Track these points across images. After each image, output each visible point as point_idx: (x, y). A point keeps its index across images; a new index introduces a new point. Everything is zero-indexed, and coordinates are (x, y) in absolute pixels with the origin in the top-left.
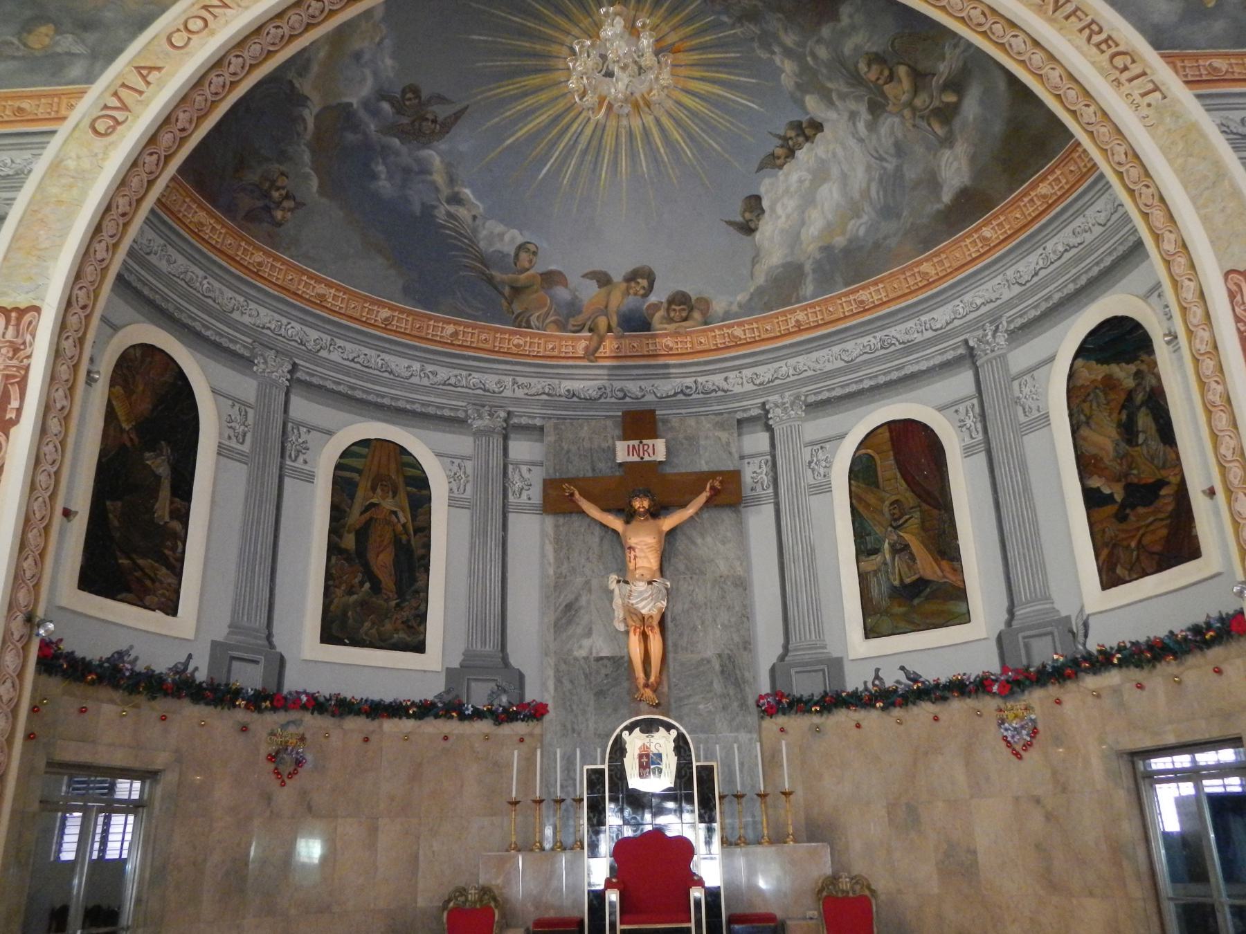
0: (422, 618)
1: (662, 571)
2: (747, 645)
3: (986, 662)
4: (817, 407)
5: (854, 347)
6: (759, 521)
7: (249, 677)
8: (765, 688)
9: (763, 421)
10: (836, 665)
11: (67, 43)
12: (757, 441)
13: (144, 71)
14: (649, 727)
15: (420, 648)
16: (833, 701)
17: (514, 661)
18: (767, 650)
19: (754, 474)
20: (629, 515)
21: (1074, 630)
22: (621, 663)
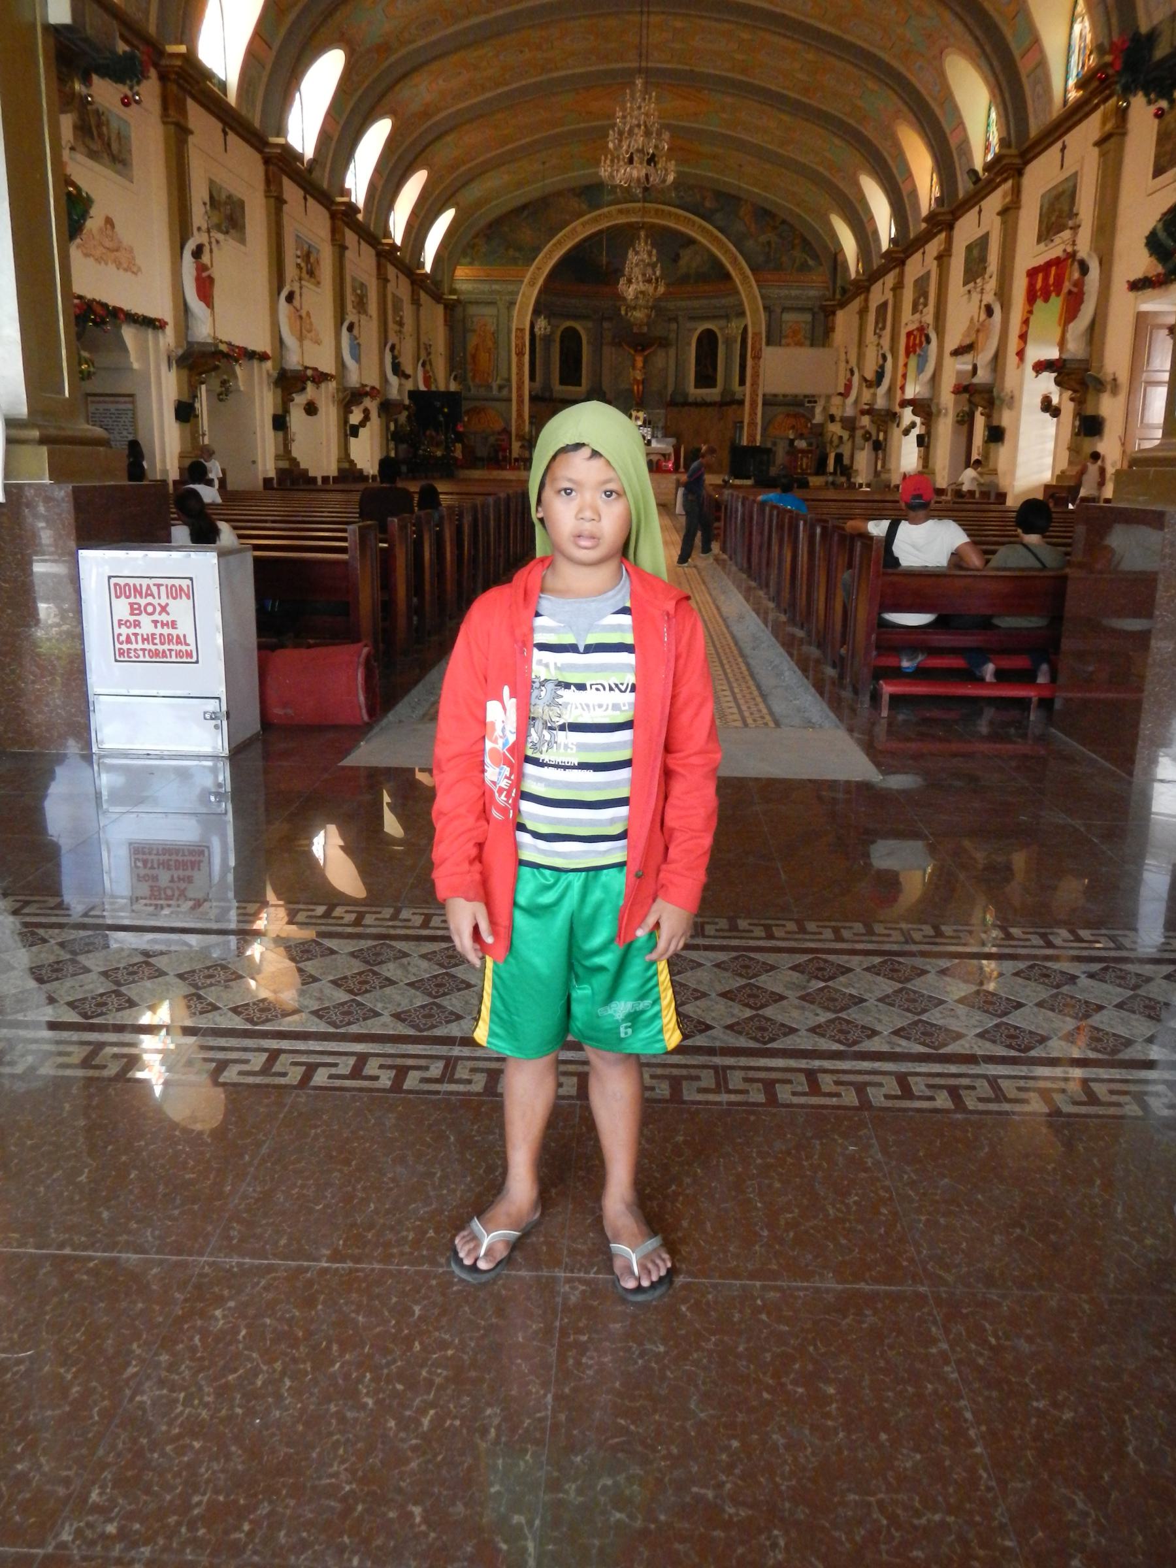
0: (580, 377)
1: (644, 367)
2: (666, 387)
3: (717, 398)
4: (692, 319)
5: (704, 302)
6: (672, 352)
7: (547, 395)
8: (669, 398)
9: (675, 319)
10: (686, 395)
11: (517, 255)
12: (674, 326)
13: (539, 269)
14: (638, 411)
15: (580, 385)
16: (686, 404)
17: (604, 388)
18: (670, 389)
19: (672, 336)
20: (636, 351)
21: (734, 393)
22: (631, 391)
